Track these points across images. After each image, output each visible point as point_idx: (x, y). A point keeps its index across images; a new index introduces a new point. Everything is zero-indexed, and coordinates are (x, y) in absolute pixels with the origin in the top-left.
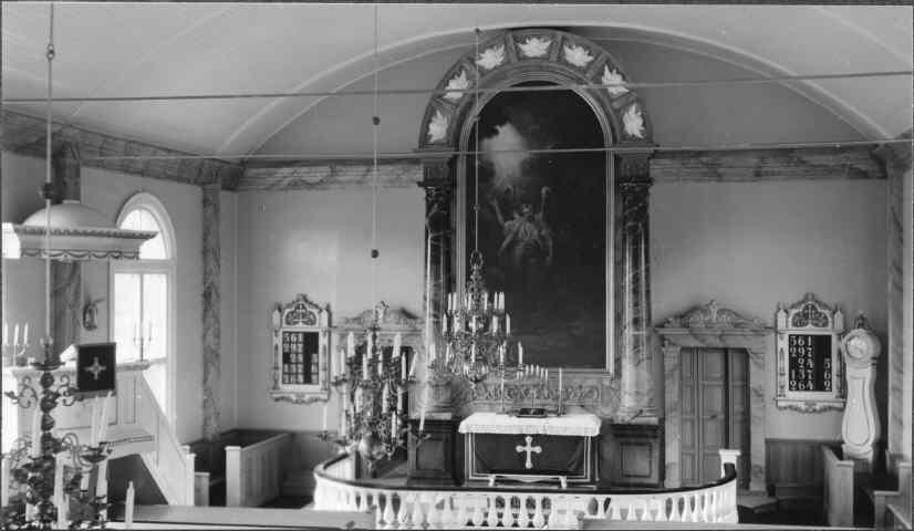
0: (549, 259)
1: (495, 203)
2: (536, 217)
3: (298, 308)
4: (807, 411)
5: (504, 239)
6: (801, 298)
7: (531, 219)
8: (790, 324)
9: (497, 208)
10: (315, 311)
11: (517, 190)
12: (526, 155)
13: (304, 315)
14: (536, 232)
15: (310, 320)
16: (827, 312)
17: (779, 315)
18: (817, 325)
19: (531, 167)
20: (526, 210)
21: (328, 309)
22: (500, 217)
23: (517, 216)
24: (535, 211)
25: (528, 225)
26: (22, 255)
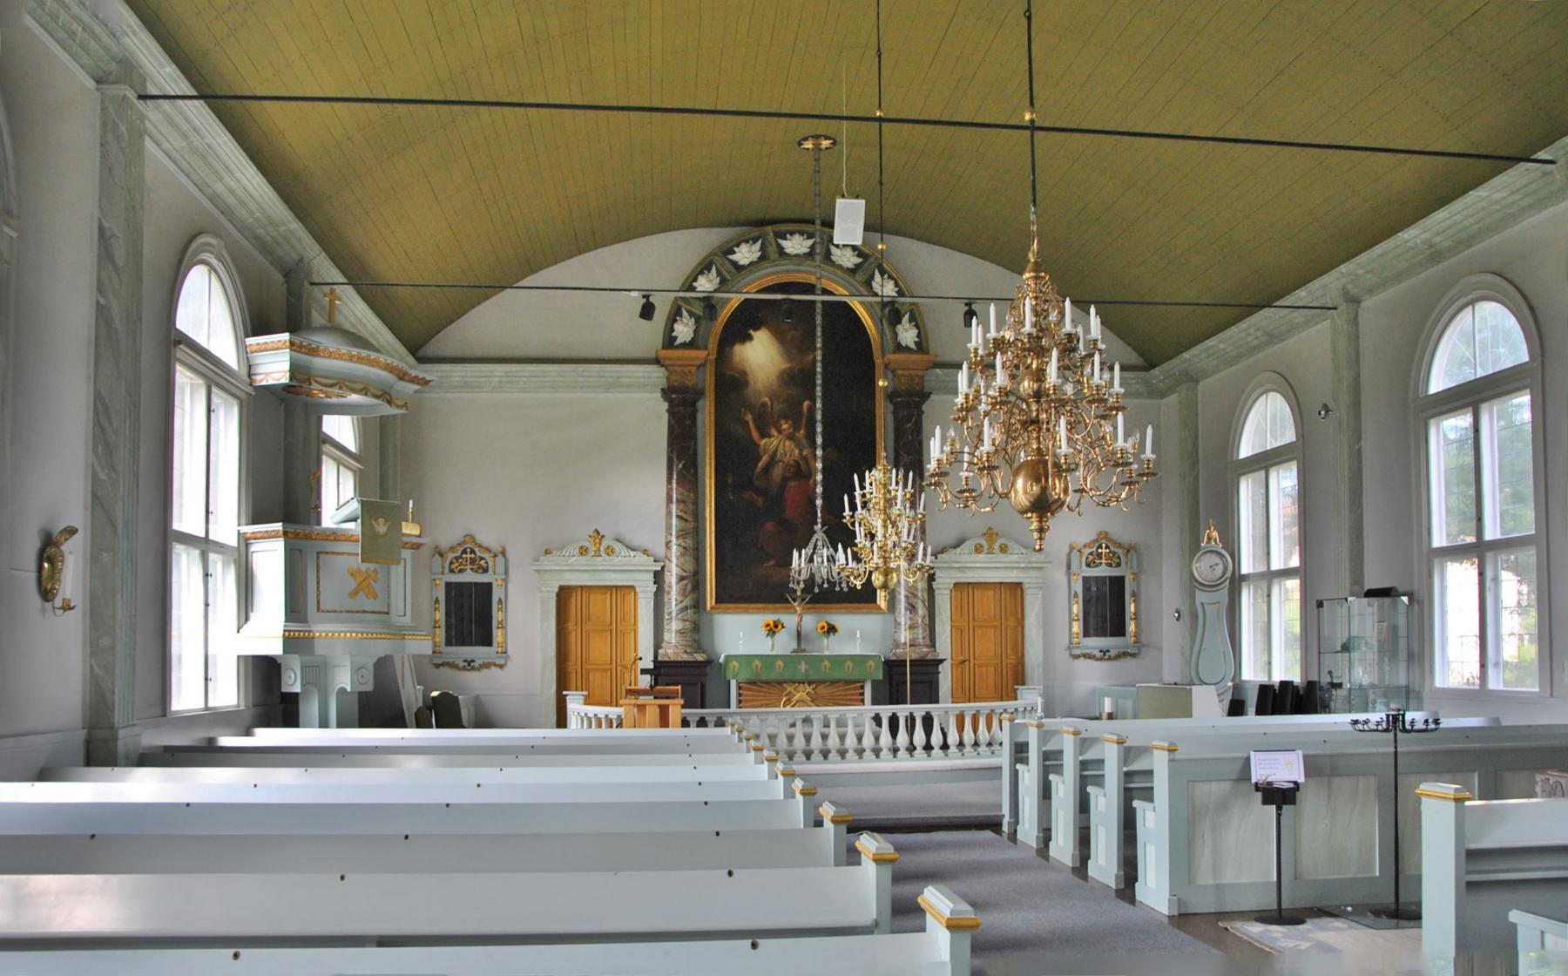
1: (749, 418)
2: (797, 434)
3: (464, 552)
4: (1101, 659)
7: (791, 437)
8: (1084, 564)
9: (751, 425)
10: (486, 555)
11: (775, 403)
12: (785, 366)
13: (473, 561)
14: (797, 451)
15: (480, 567)
16: (1120, 551)
17: (1072, 554)
18: (1110, 565)
20: (785, 426)
21: (503, 553)
22: (755, 435)
23: (774, 432)
25: (787, 442)
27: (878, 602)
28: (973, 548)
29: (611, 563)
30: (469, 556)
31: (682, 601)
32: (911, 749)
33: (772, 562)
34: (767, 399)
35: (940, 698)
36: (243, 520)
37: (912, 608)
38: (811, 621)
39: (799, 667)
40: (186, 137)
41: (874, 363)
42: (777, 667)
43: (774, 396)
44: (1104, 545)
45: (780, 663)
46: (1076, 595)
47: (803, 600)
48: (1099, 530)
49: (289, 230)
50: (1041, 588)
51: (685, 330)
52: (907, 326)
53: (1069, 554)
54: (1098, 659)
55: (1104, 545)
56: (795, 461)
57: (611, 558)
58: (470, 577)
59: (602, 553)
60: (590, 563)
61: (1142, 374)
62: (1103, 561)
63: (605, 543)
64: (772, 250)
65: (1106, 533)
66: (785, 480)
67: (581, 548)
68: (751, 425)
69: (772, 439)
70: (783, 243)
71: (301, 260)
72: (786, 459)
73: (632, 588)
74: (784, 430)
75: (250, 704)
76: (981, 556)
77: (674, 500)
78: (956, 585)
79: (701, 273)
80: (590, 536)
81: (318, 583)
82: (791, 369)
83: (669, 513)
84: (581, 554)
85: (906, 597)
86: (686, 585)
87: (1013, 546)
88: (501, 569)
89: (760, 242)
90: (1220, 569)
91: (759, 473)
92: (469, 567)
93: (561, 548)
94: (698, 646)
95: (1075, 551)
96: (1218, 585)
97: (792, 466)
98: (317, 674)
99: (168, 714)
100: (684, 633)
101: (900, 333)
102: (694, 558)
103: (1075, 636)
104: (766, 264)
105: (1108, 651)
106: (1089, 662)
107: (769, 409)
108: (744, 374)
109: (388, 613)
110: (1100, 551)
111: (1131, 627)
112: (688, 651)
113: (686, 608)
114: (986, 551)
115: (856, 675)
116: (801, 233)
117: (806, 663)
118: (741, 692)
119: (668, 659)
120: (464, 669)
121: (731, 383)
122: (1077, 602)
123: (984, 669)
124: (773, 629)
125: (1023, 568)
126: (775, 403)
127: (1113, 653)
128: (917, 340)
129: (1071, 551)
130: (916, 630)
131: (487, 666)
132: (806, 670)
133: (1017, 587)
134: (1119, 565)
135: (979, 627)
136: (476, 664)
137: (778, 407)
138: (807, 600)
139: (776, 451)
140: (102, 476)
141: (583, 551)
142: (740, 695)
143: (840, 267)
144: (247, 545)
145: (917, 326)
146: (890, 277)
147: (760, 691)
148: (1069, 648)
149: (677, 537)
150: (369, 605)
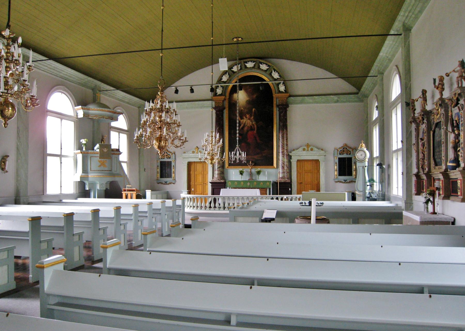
0: (255, 132)
6: (342, 145)
7: (249, 119)
8: (339, 154)
10: (170, 154)
12: (248, 99)
13: (167, 155)
14: (251, 123)
16: (351, 150)
18: (347, 154)
19: (248, 102)
20: (248, 116)
21: (175, 154)
24: (251, 116)
25: (248, 121)
26: (83, 116)
28: (302, 150)
30: (166, 154)
35: (292, 193)
36: (75, 149)
37: (283, 167)
38: (254, 170)
40: (47, 66)
41: (273, 97)
43: (245, 108)
44: (345, 148)
45: (262, 183)
46: (336, 163)
48: (345, 143)
49: (88, 80)
50: (324, 161)
51: (219, 91)
52: (282, 85)
53: (334, 151)
54: (343, 183)
55: (345, 148)
58: (166, 160)
61: (356, 95)
62: (345, 153)
65: (346, 144)
66: (248, 131)
67: (193, 151)
70: (246, 64)
71: (96, 86)
72: (248, 125)
75: (78, 192)
79: (224, 75)
81: (91, 164)
84: (193, 153)
85: (281, 164)
87: (315, 149)
88: (174, 157)
90: (364, 155)
92: (166, 157)
93: (187, 152)
94: (223, 178)
96: (363, 161)
97: (249, 127)
98: (93, 185)
99: (45, 194)
101: (280, 88)
102: (222, 154)
104: (241, 71)
105: (347, 180)
106: (341, 184)
109: (111, 171)
110: (344, 150)
111: (354, 173)
115: (265, 187)
116: (251, 61)
120: (165, 184)
121: (233, 105)
123: (307, 185)
124: (241, 173)
125: (318, 155)
127: (348, 181)
128: (285, 89)
129: (335, 150)
131: (170, 183)
132: (250, 185)
133: (317, 161)
134: (350, 154)
135: (306, 173)
136: (167, 183)
137: (246, 111)
139: (245, 123)
140: (18, 144)
141: (193, 152)
143: (263, 70)
144: (76, 155)
145: (285, 85)
146: (277, 72)
148: (334, 179)
150: (106, 169)
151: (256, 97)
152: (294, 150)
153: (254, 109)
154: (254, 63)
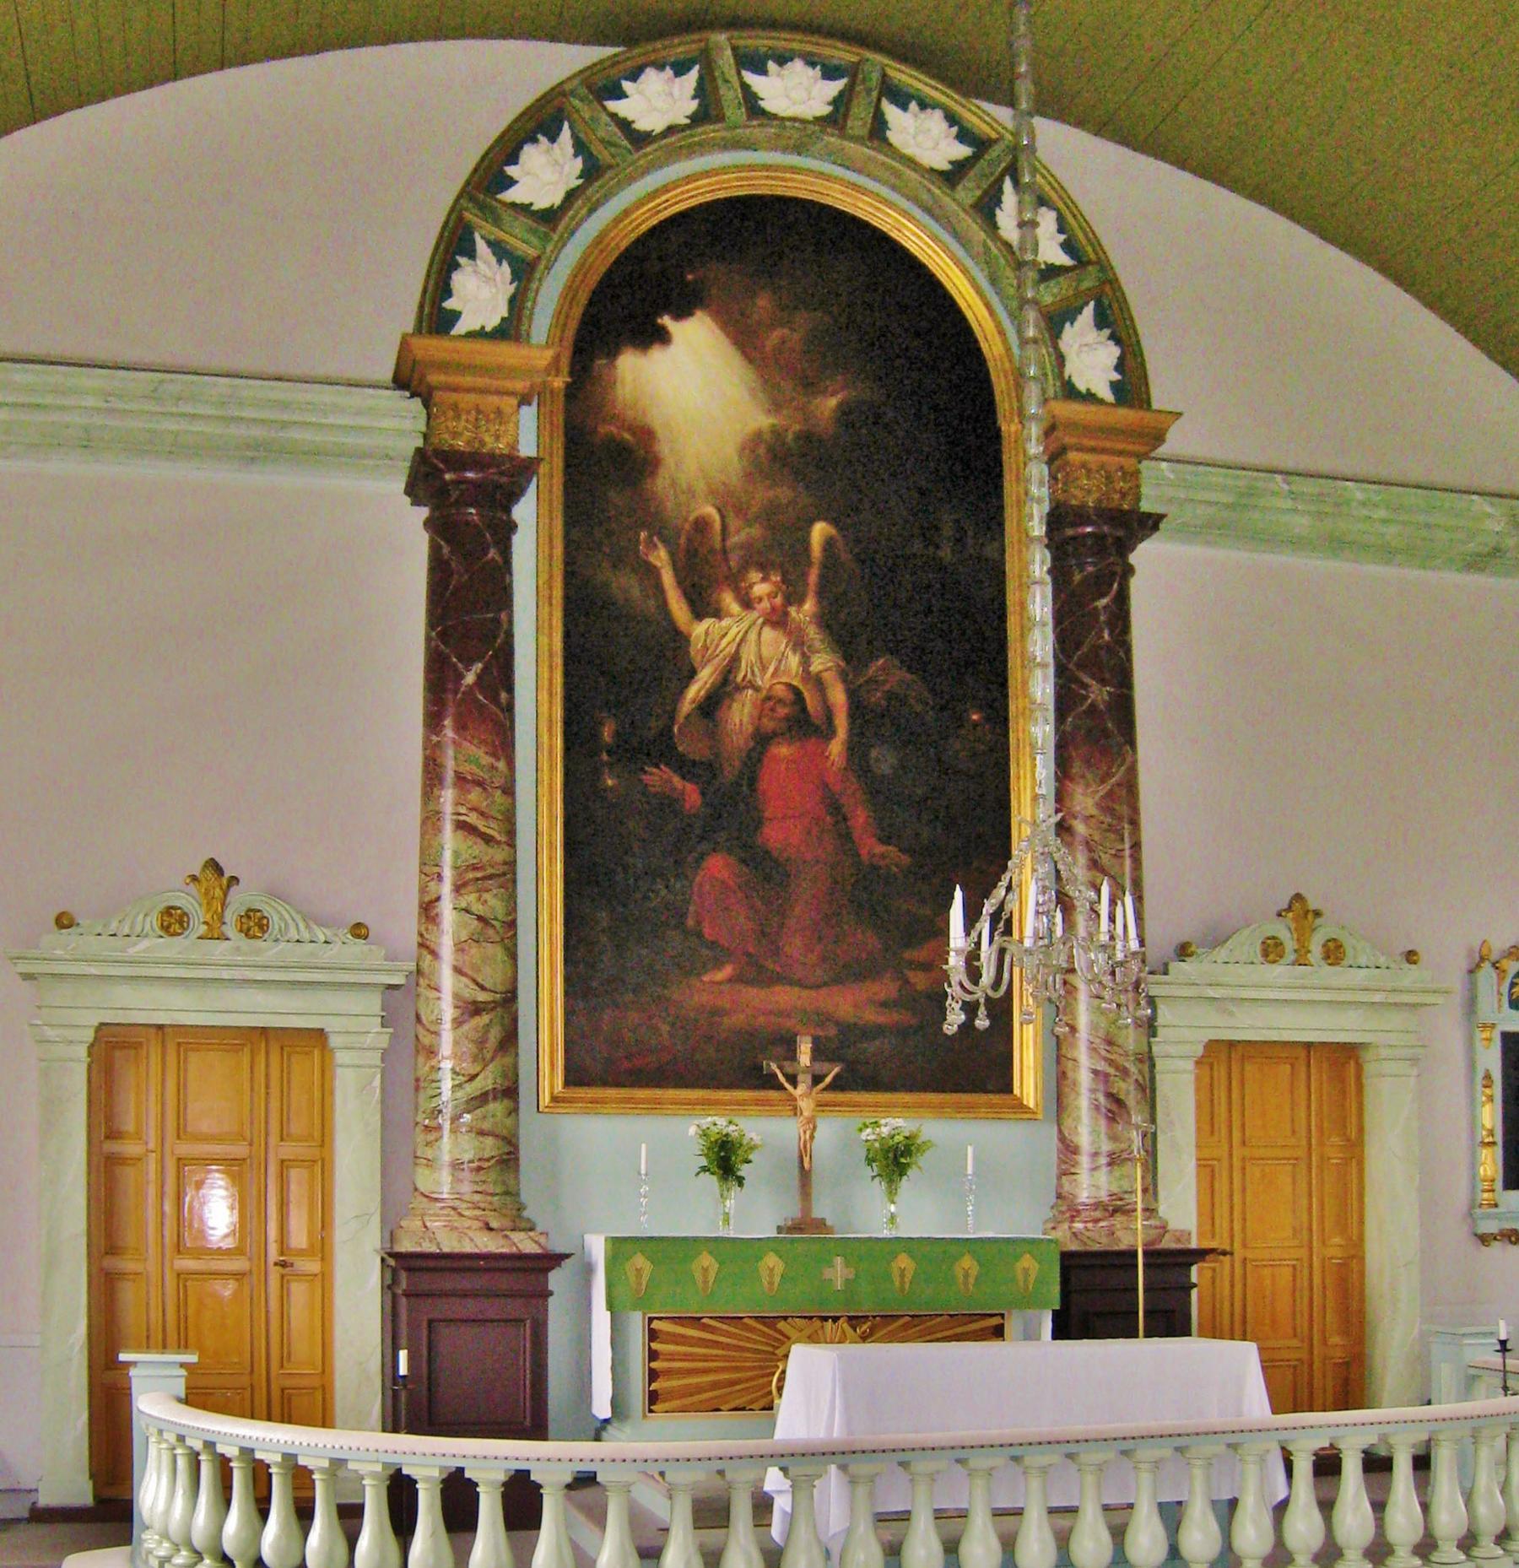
1: (660, 558)
2: (793, 610)
5: (692, 673)
7: (778, 620)
9: (668, 578)
12: (763, 420)
14: (794, 661)
20: (760, 589)
25: (768, 634)
27: (1016, 1091)
29: (259, 960)
31: (472, 1078)
32: (1172, 1515)
33: (727, 971)
34: (710, 511)
39: (828, 1273)
42: (764, 1274)
47: (817, 1079)
56: (789, 686)
57: (259, 943)
59: (231, 930)
60: (194, 957)
63: (239, 900)
64: (730, 96)
67: (169, 911)
68: (668, 578)
69: (725, 622)
73: (318, 1036)
74: (760, 600)
76: (1279, 972)
77: (449, 776)
78: (1213, 1046)
80: (194, 878)
82: (777, 433)
83: (431, 821)
86: (488, 1026)
89: (694, 74)
91: (688, 717)
95: (1487, 965)
100: (479, 1169)
103: (1486, 1185)
107: (718, 538)
108: (646, 434)
112: (494, 1224)
113: (483, 1099)
114: (1291, 957)
117: (847, 1264)
118: (654, 1346)
119: (433, 1249)
122: (1491, 1099)
126: (733, 522)
130: (1126, 1169)
137: (743, 534)
138: (828, 1079)
139: (735, 659)
141: (173, 921)
142: (653, 1355)
145: (1115, 338)
147: (716, 1344)
149: (458, 889)
151: (845, 413)
152: (1183, 952)
153: (820, 531)
154: (834, 88)
